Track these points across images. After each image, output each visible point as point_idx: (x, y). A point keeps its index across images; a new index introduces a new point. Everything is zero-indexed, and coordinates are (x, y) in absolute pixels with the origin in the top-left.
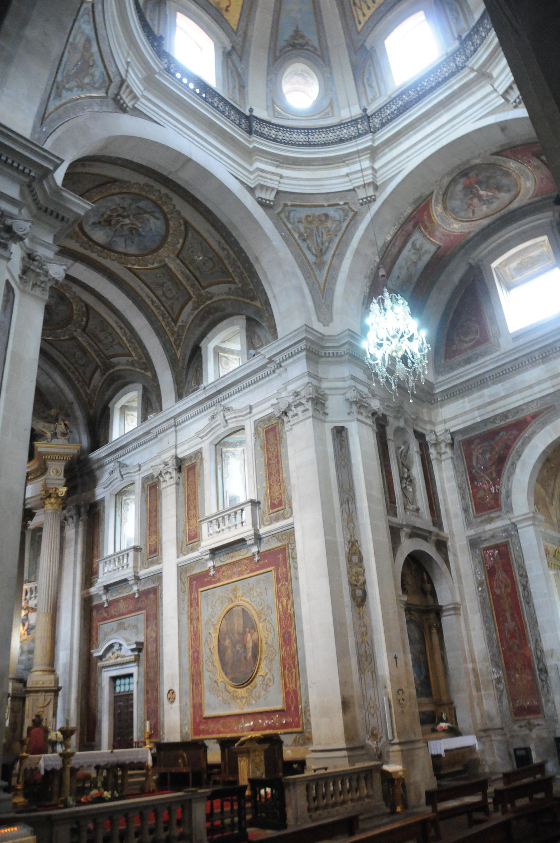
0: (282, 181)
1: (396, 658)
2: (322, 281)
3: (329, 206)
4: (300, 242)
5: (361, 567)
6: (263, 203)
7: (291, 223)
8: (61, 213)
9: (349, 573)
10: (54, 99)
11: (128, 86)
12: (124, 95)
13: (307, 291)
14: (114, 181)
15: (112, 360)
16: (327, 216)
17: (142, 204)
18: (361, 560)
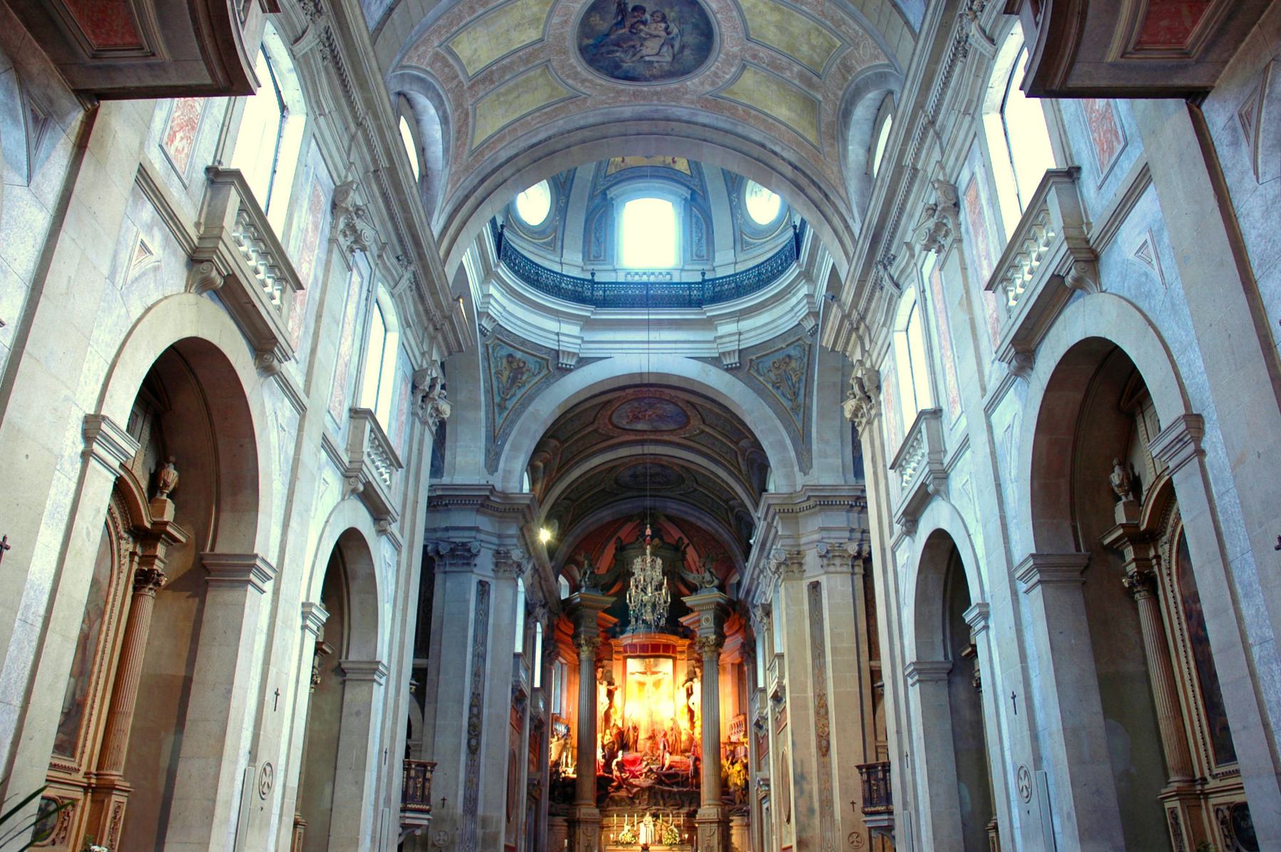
0: (742, 337)
1: (853, 803)
2: (800, 425)
3: (788, 346)
4: (774, 391)
5: (827, 719)
6: (729, 369)
7: (761, 375)
8: (515, 507)
9: (816, 725)
10: (500, 414)
11: (563, 352)
12: (564, 361)
13: (788, 442)
14: (609, 402)
15: (731, 503)
16: (789, 356)
17: (646, 401)
18: (827, 712)
